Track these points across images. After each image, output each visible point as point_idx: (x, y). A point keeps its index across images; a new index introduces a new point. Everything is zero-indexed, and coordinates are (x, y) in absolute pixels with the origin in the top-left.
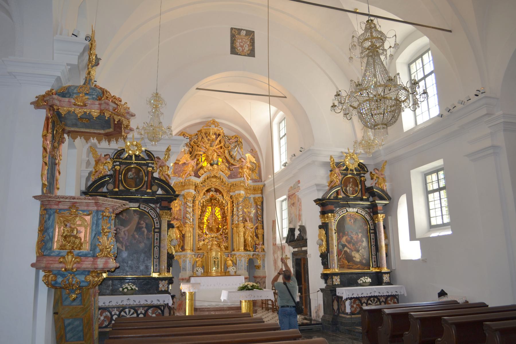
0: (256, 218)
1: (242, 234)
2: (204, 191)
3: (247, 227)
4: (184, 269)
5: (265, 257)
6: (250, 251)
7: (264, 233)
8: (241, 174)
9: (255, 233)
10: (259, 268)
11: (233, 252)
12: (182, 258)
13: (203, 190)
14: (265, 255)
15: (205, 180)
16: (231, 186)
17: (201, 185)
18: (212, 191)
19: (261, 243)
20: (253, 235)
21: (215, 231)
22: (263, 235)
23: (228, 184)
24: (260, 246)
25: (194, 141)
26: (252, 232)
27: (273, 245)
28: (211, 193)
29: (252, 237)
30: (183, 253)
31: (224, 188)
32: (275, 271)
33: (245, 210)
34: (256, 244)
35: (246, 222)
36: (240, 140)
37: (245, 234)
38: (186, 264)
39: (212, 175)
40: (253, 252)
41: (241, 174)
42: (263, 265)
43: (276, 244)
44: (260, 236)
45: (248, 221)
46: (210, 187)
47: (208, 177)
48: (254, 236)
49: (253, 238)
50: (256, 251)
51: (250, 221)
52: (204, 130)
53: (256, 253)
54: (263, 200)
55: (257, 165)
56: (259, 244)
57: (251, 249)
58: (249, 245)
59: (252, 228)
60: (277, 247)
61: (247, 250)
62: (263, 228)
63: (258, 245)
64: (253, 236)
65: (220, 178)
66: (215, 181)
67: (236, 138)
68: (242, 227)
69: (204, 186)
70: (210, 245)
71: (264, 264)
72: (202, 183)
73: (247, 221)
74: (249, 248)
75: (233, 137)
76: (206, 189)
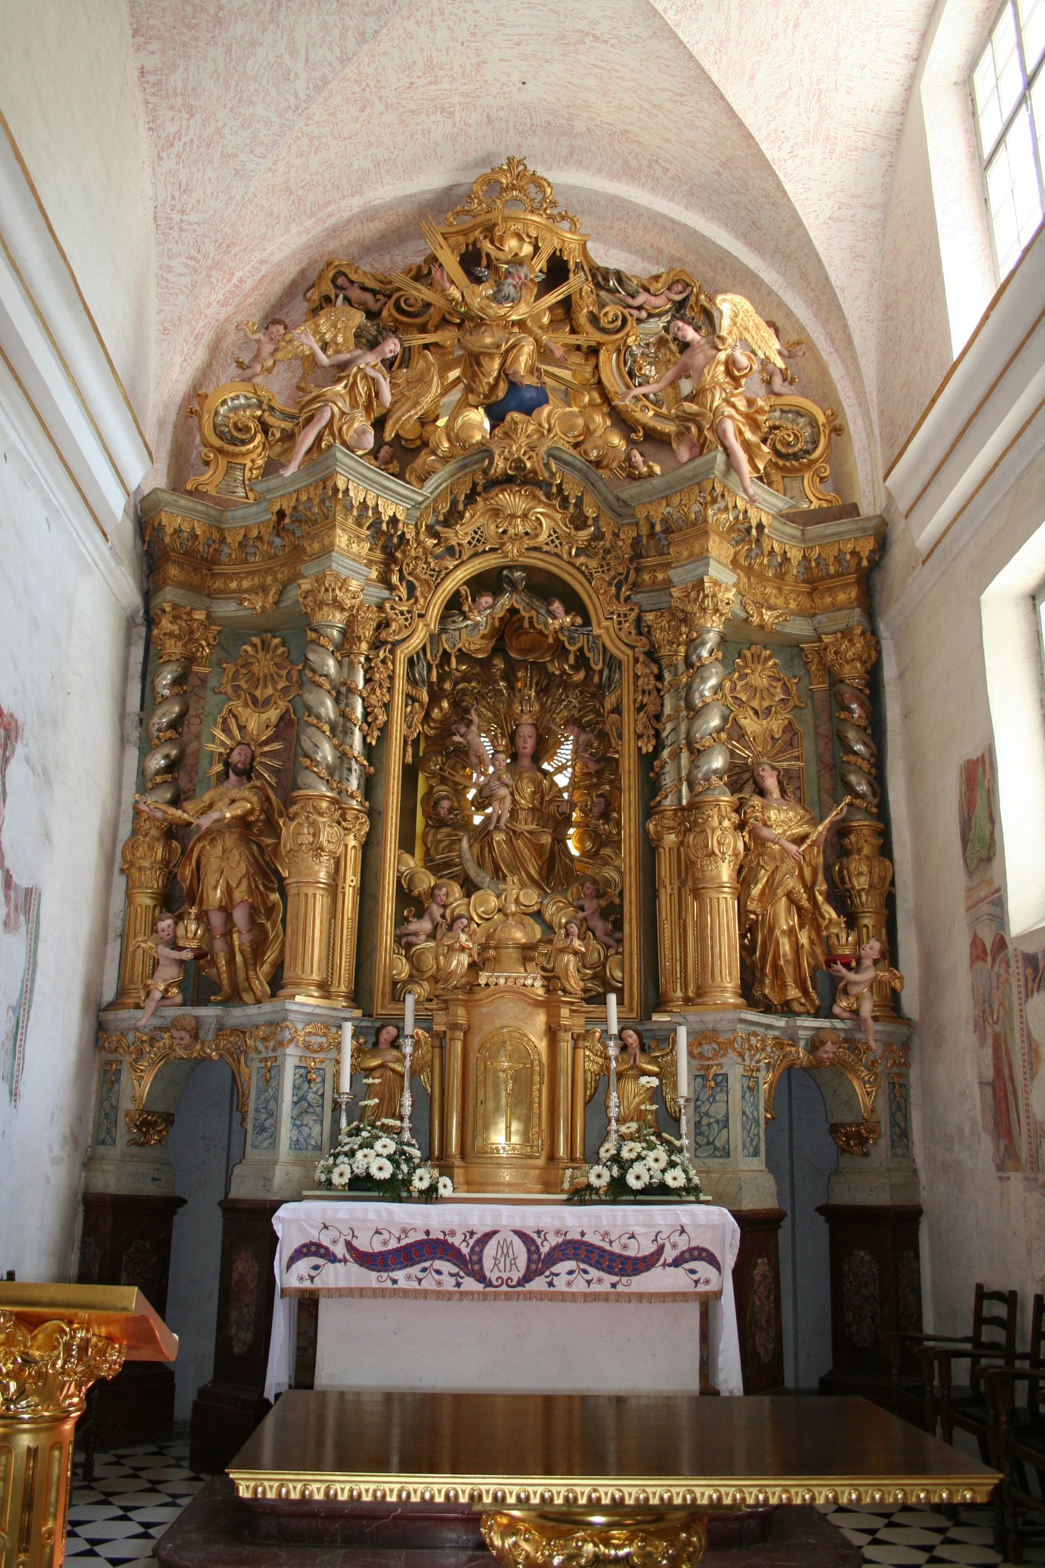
0: (827, 781)
1: (725, 872)
2: (449, 586)
3: (765, 832)
4: (264, 1129)
5: (907, 1065)
6: (786, 1009)
7: (892, 883)
8: (694, 429)
9: (829, 880)
10: (863, 1141)
11: (656, 1017)
12: (260, 1046)
13: (442, 575)
14: (906, 1045)
15: (454, 503)
16: (636, 541)
17: (430, 542)
18: (513, 585)
19: (873, 948)
20: (810, 891)
21: (536, 877)
22: (890, 902)
23: (616, 535)
24: (868, 974)
25: (398, 300)
26: (807, 872)
27: (978, 952)
28: (505, 601)
29: (805, 904)
30: (267, 1007)
31: (593, 564)
32: (1000, 1168)
33: (750, 724)
34: (830, 961)
35: (756, 801)
36: (703, 297)
37: (744, 877)
38: (276, 1100)
39: (500, 464)
40: (816, 1015)
41: (694, 429)
42: (894, 1123)
43: (1001, 943)
44: (868, 904)
45: (776, 794)
46: (489, 561)
47: (475, 485)
48: (820, 898)
49: (809, 917)
50: (836, 1010)
51: (783, 792)
52: (461, 239)
53: (838, 1024)
54: (879, 652)
55: (821, 419)
56: (859, 960)
57: (793, 993)
58: (776, 969)
59: (800, 840)
60: (1017, 967)
61: (768, 1008)
62: (885, 850)
63: (847, 965)
64: (812, 898)
65: (565, 502)
66: (525, 516)
67: (680, 288)
68: (726, 823)
69: (451, 551)
70: (463, 949)
71: (899, 1116)
72: (436, 535)
73: (762, 792)
74: (783, 987)
75: (656, 278)
76: (462, 574)
